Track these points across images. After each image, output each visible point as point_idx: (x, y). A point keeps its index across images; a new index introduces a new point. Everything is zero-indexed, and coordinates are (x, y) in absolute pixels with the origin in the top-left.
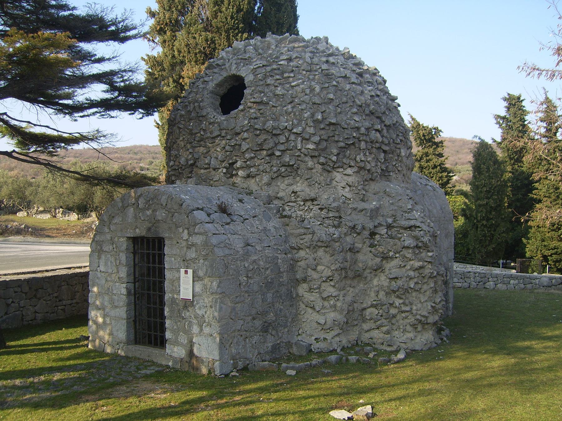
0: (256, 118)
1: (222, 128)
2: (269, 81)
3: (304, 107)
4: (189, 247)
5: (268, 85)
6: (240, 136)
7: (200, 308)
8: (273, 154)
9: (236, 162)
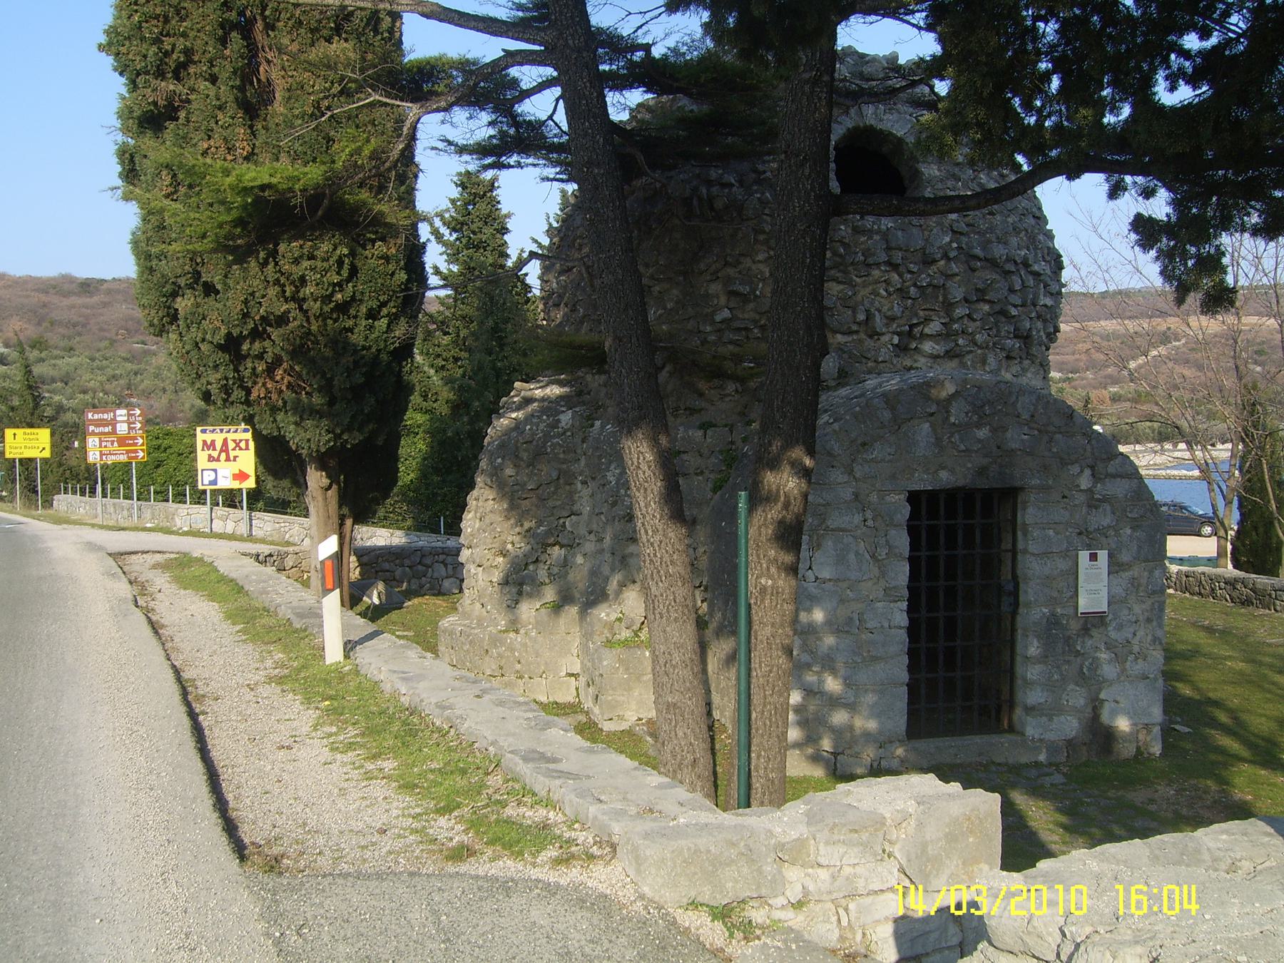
1: (893, 245)
4: (1094, 503)
6: (934, 268)
7: (1120, 627)
8: (1003, 313)
9: (927, 320)
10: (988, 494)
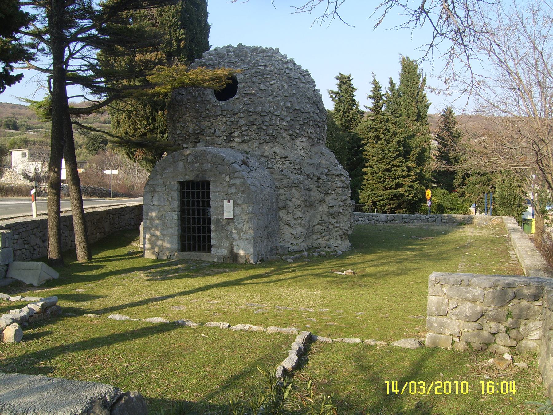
0: (248, 104)
2: (254, 80)
3: (280, 98)
4: (230, 186)
5: (254, 82)
7: (239, 223)
8: (261, 128)
9: (234, 132)
10: (203, 182)
